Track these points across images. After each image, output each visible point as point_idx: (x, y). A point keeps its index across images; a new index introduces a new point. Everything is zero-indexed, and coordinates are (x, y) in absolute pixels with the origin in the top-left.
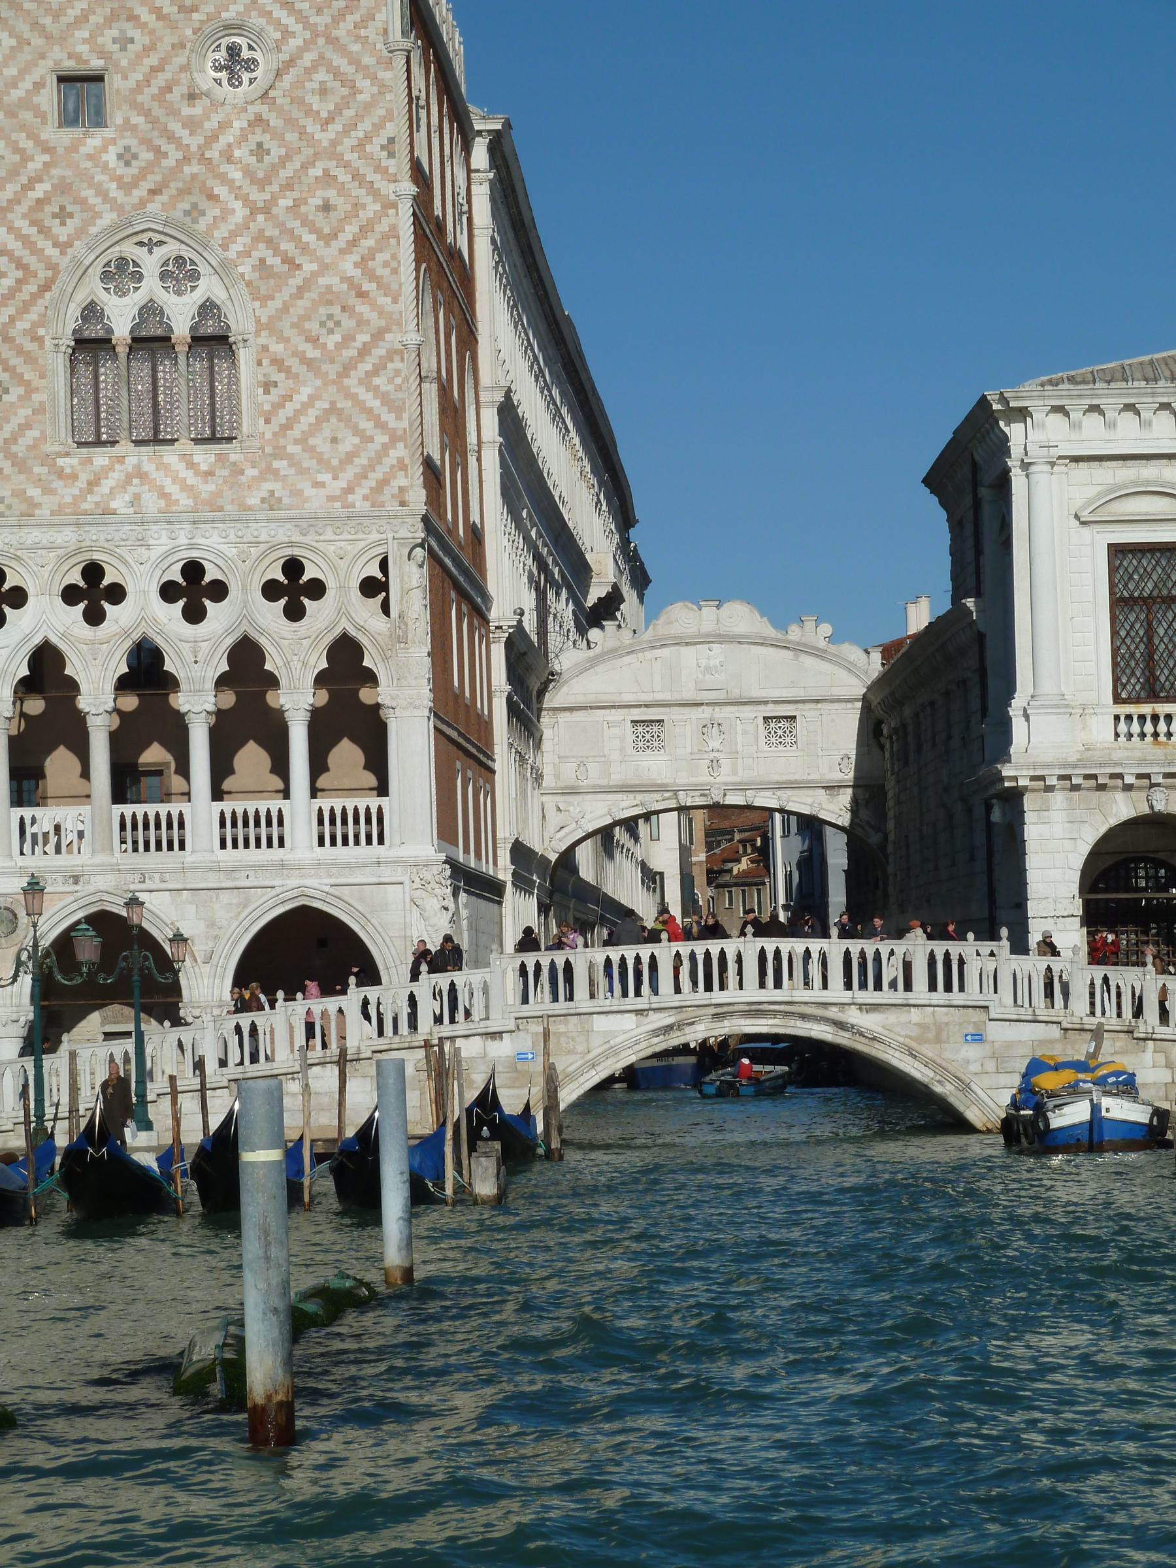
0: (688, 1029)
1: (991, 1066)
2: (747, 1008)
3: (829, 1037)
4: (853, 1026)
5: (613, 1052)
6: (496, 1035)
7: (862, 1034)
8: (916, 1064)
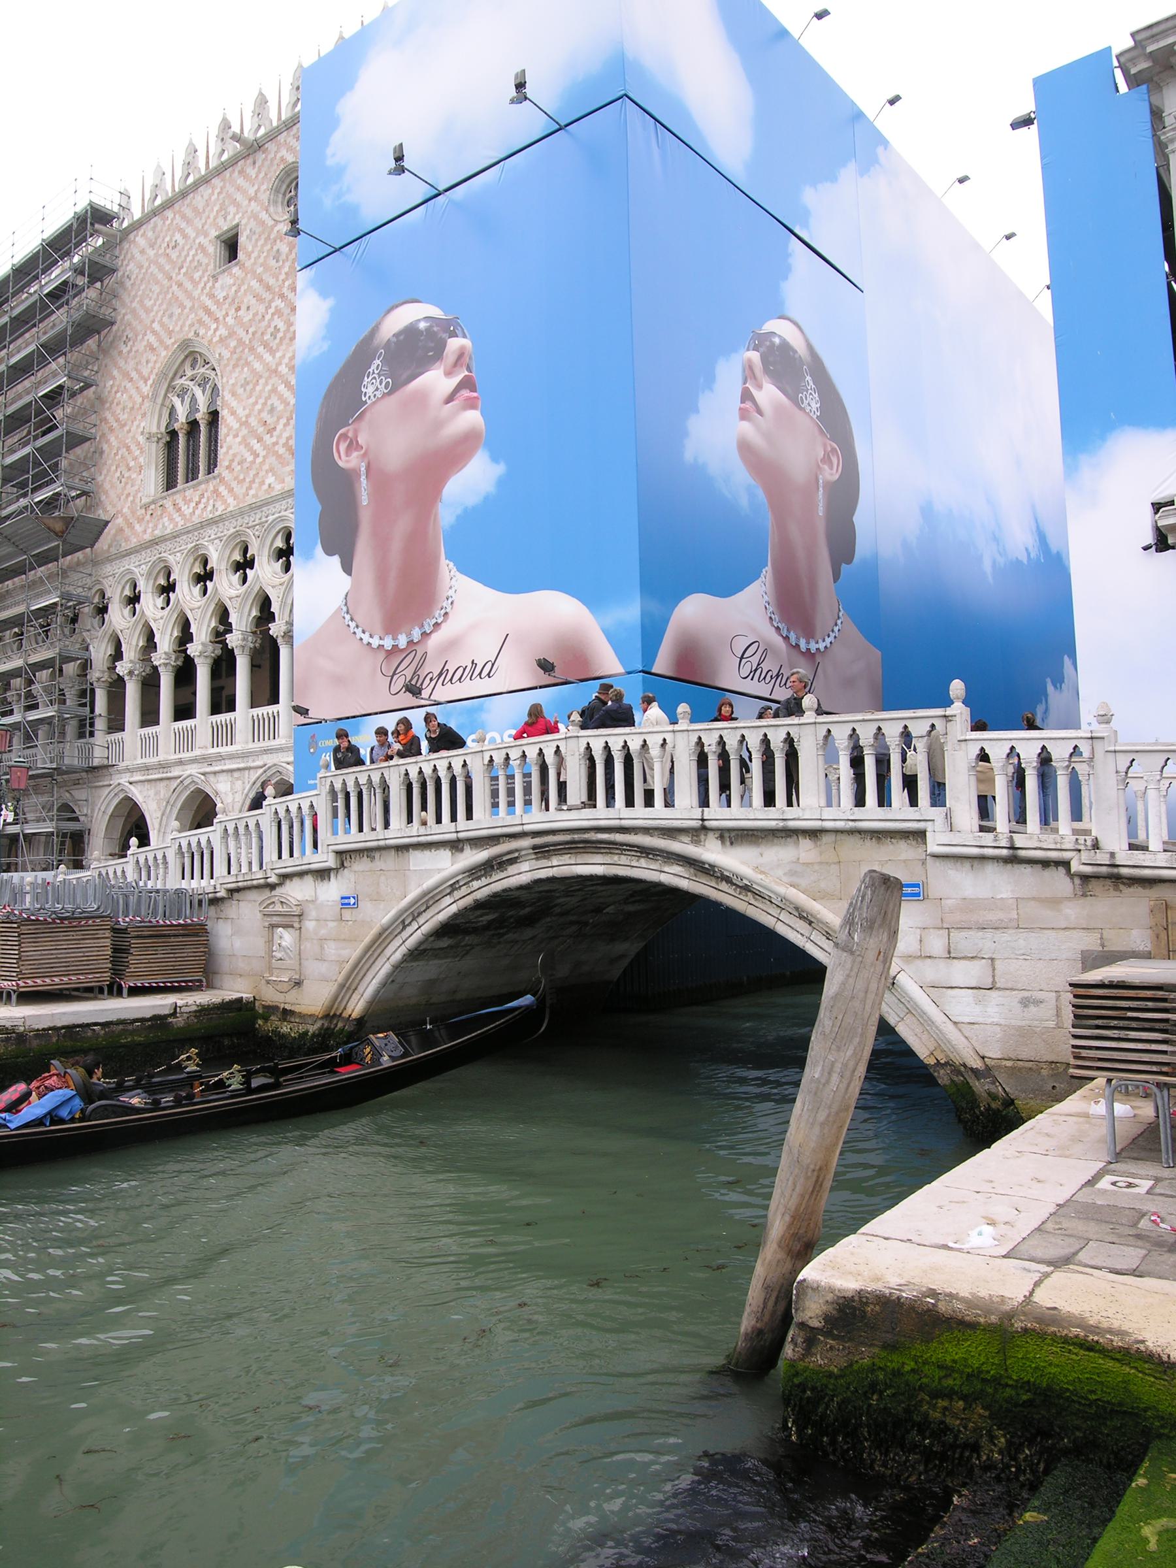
0: (512, 870)
1: (936, 944)
2: (567, 838)
3: (684, 884)
4: (712, 866)
5: (429, 899)
6: (323, 874)
7: (728, 880)
8: (816, 936)
